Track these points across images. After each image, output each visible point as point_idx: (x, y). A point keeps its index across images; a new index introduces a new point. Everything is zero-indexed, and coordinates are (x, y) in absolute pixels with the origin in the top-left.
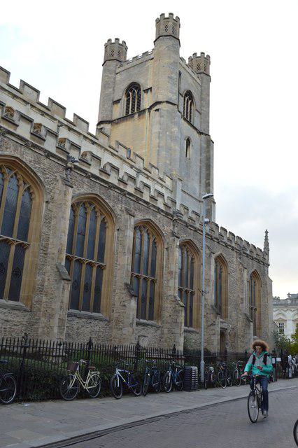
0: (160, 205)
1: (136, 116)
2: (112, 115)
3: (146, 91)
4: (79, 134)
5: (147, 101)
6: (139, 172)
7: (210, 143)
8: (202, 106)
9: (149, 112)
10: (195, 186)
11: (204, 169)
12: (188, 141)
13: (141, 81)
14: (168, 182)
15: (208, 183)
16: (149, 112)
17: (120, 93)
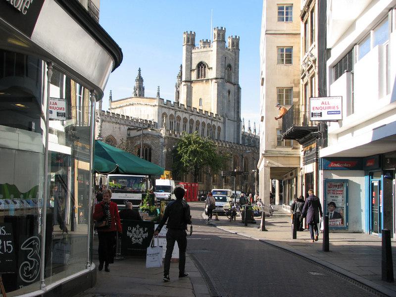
0: (228, 147)
1: (204, 81)
2: (191, 77)
3: (209, 69)
4: (195, 115)
5: (212, 74)
6: (212, 120)
7: (239, 89)
8: (235, 68)
9: (212, 81)
10: (232, 114)
11: (236, 104)
12: (229, 92)
13: (206, 61)
14: (222, 119)
15: (238, 112)
16: (212, 81)
17: (194, 66)
